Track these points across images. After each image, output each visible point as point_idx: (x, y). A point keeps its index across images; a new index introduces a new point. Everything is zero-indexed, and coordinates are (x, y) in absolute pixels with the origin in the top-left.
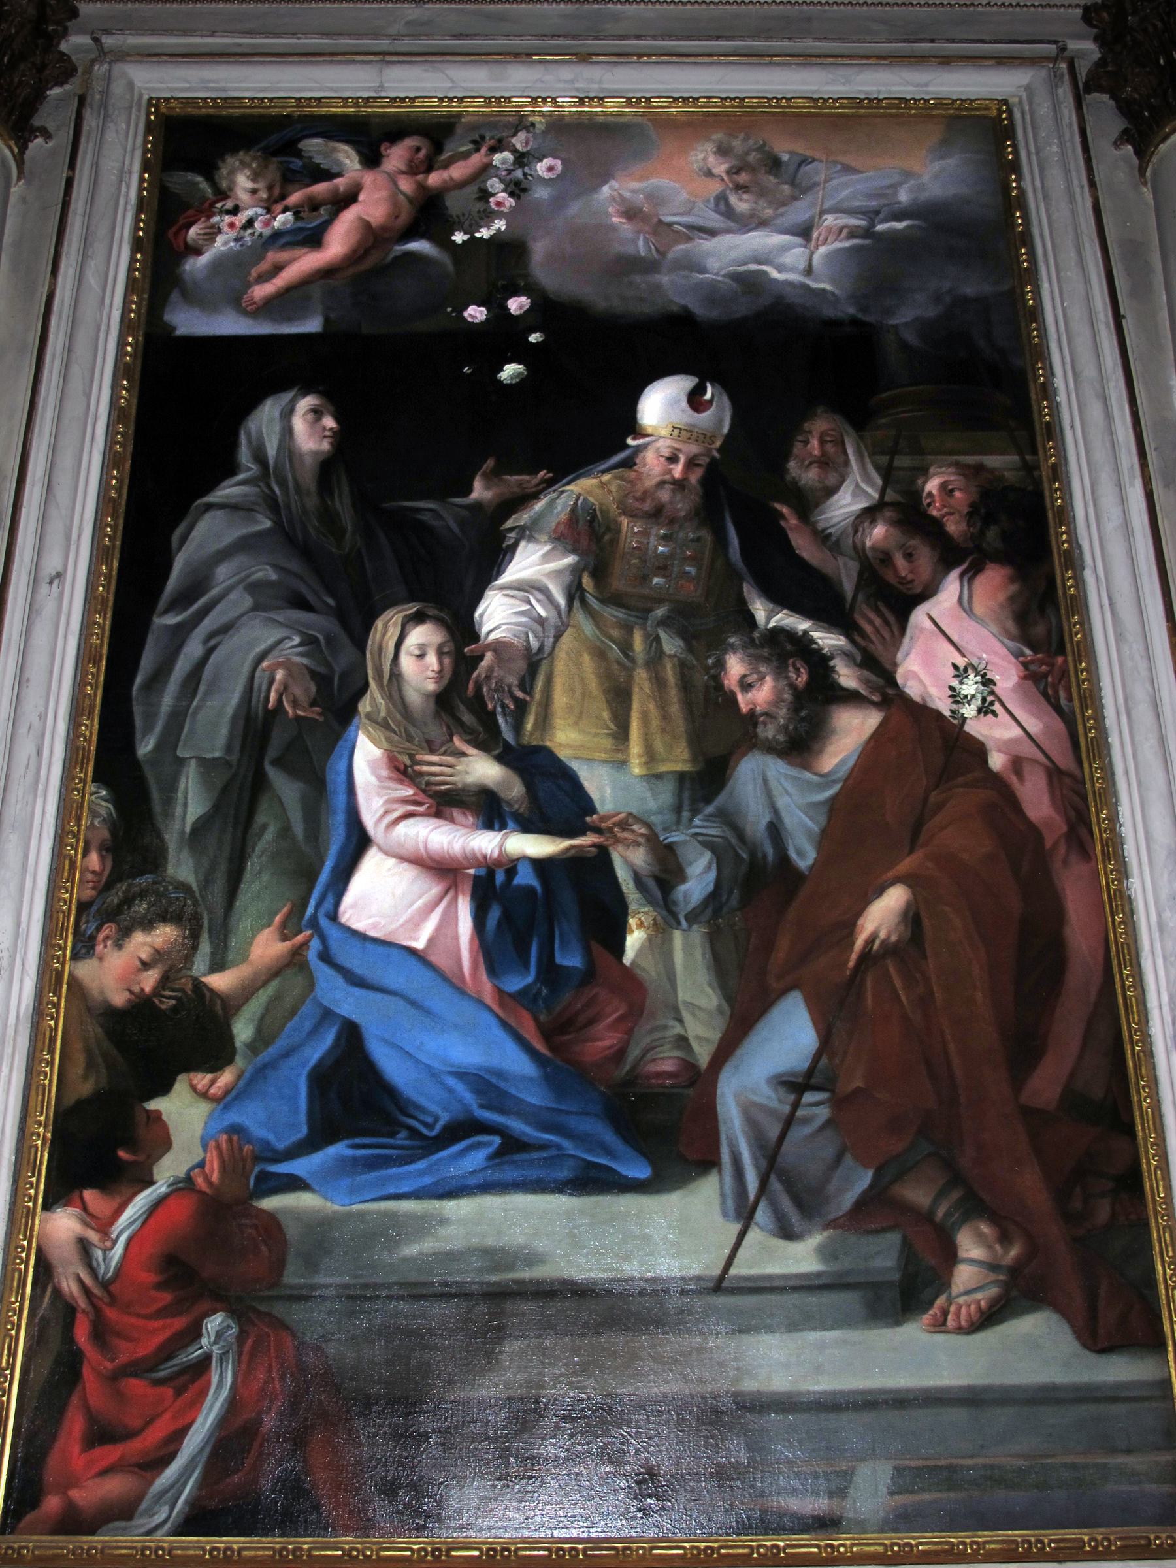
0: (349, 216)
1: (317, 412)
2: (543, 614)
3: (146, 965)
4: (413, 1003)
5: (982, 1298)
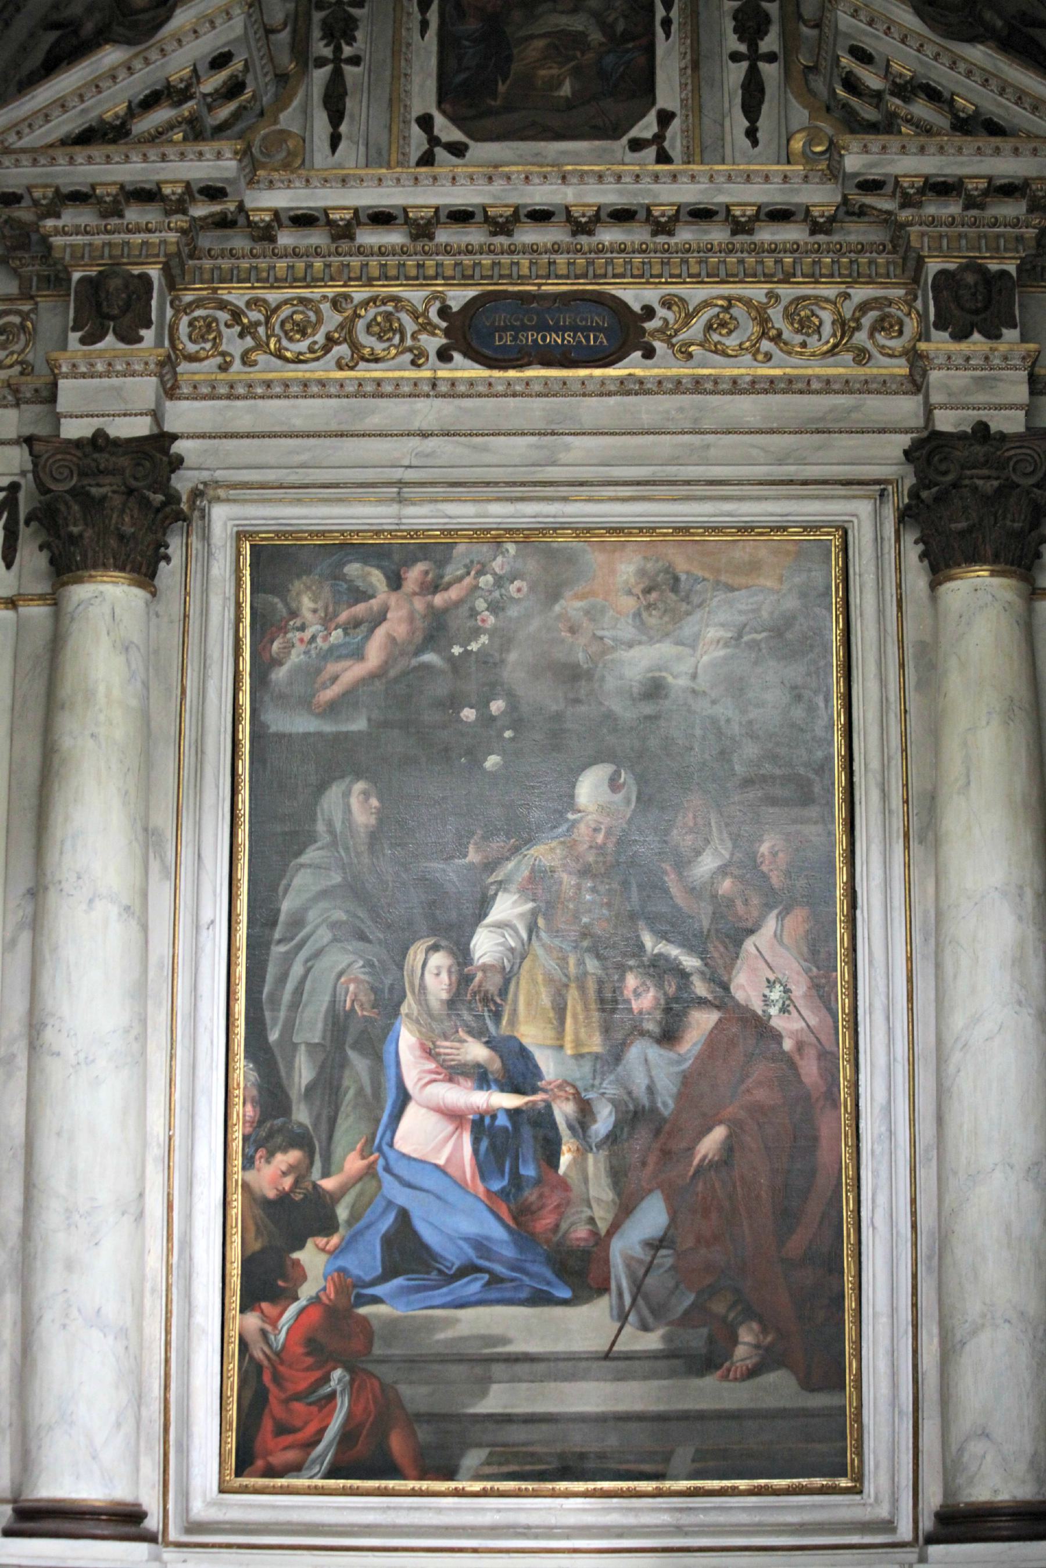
0: (381, 632)
1: (366, 794)
2: (513, 944)
3: (284, 1174)
4: (438, 1197)
5: (749, 1363)
